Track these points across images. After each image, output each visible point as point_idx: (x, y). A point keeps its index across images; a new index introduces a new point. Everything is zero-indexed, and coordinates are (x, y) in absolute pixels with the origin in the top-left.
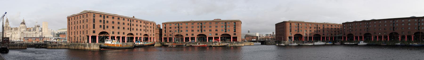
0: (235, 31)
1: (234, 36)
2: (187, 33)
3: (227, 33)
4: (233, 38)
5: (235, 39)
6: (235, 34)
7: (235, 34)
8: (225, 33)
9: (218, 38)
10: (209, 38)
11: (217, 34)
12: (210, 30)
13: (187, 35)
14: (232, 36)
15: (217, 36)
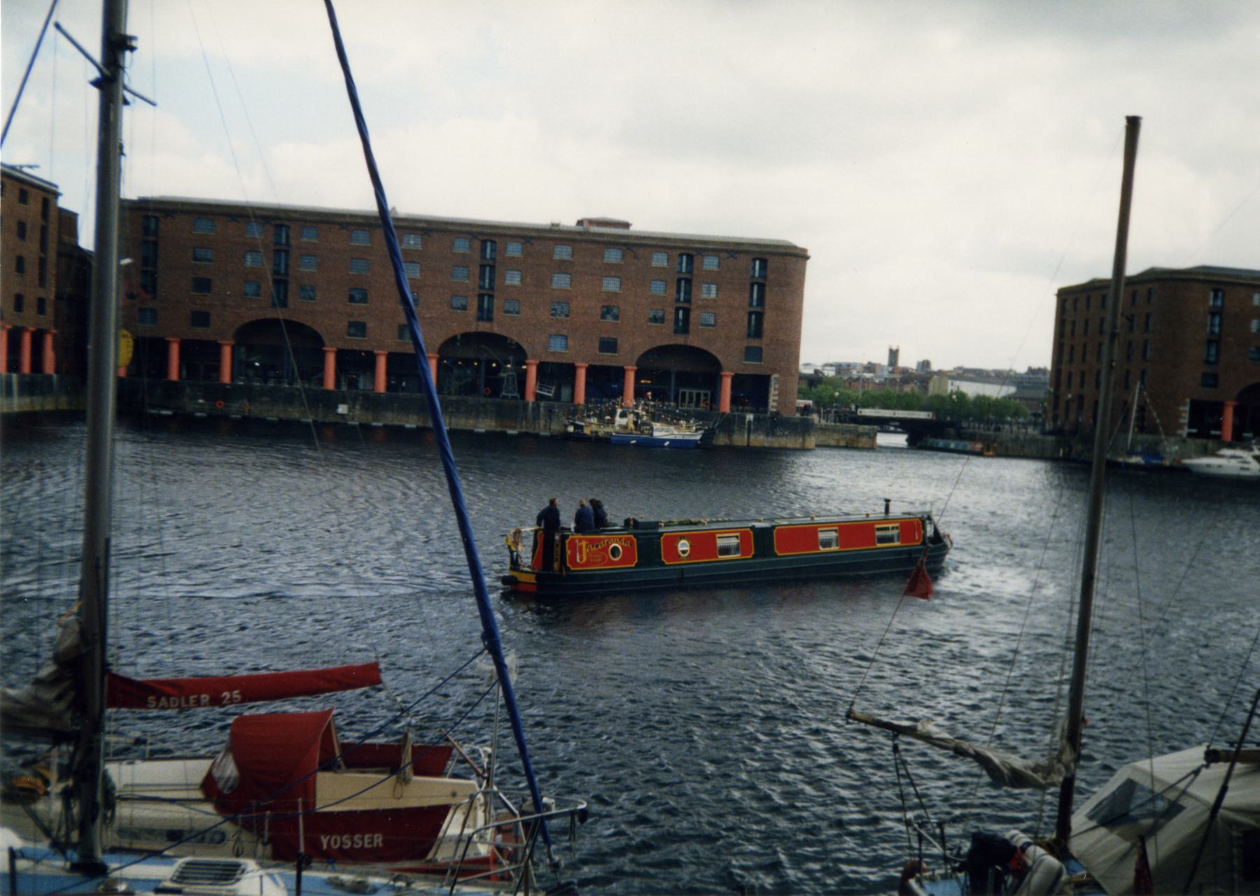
0: (756, 330)
1: (751, 367)
2: (359, 311)
3: (694, 340)
4: (738, 381)
5: (753, 390)
6: (754, 353)
7: (754, 353)
8: (680, 340)
9: (620, 372)
10: (541, 367)
11: (609, 345)
12: (203, 285)
13: (359, 328)
14: (732, 365)
15: (608, 359)
